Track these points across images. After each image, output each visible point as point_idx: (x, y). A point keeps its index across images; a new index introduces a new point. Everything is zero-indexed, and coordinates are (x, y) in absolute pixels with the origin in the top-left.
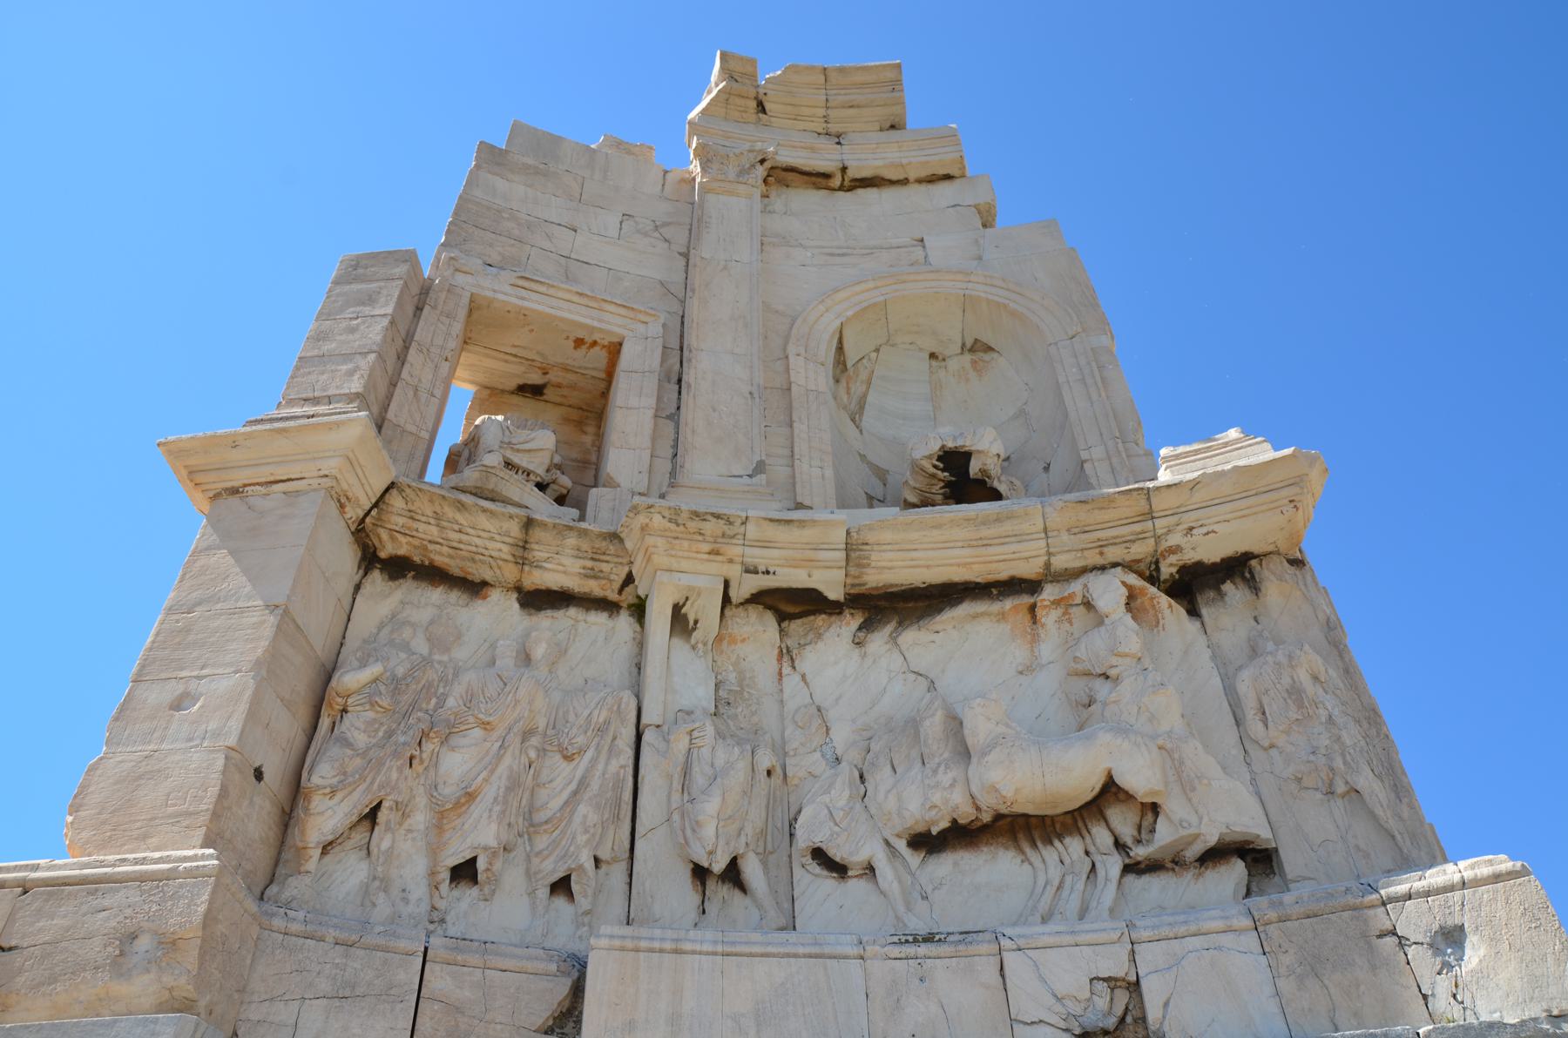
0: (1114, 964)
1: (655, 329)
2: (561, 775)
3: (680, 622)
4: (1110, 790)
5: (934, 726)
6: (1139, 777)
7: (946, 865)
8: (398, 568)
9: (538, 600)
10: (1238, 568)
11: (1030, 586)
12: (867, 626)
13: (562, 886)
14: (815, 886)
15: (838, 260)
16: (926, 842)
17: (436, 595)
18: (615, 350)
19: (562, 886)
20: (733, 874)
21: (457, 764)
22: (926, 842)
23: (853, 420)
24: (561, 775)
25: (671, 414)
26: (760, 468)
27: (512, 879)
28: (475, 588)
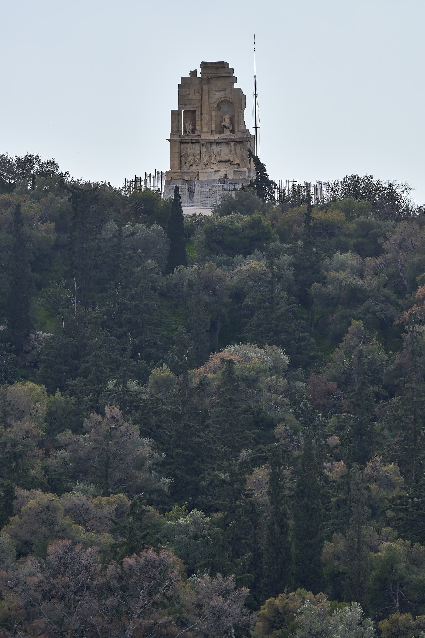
0: (226, 173)
1: (199, 109)
2: (196, 158)
3: (203, 145)
4: (229, 160)
5: (220, 154)
6: (231, 160)
7: (220, 163)
8: (183, 143)
9: (193, 143)
10: (242, 141)
11: (228, 142)
12: (217, 144)
13: (197, 165)
14: (212, 164)
15: (217, 93)
16: (219, 162)
17: (185, 145)
18: (196, 111)
19: (197, 165)
20: (207, 164)
21: (190, 159)
22: (219, 162)
23: (220, 110)
24: (196, 158)
25: (201, 120)
26: (209, 129)
27: (194, 165)
28: (188, 143)
